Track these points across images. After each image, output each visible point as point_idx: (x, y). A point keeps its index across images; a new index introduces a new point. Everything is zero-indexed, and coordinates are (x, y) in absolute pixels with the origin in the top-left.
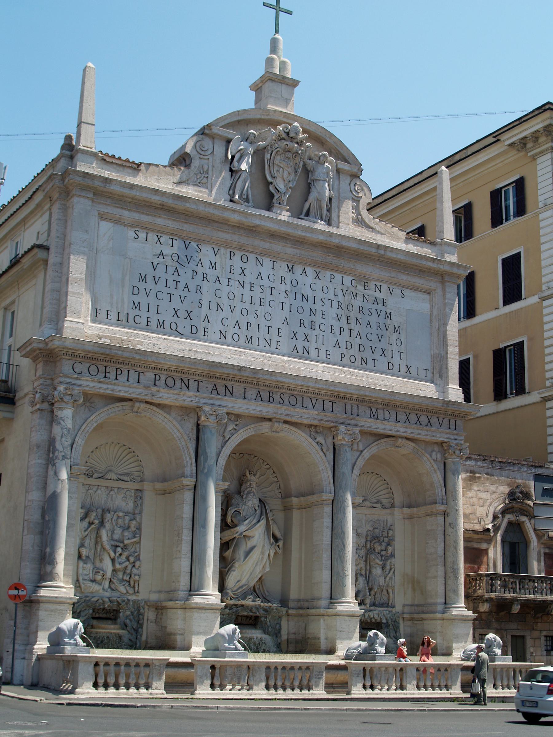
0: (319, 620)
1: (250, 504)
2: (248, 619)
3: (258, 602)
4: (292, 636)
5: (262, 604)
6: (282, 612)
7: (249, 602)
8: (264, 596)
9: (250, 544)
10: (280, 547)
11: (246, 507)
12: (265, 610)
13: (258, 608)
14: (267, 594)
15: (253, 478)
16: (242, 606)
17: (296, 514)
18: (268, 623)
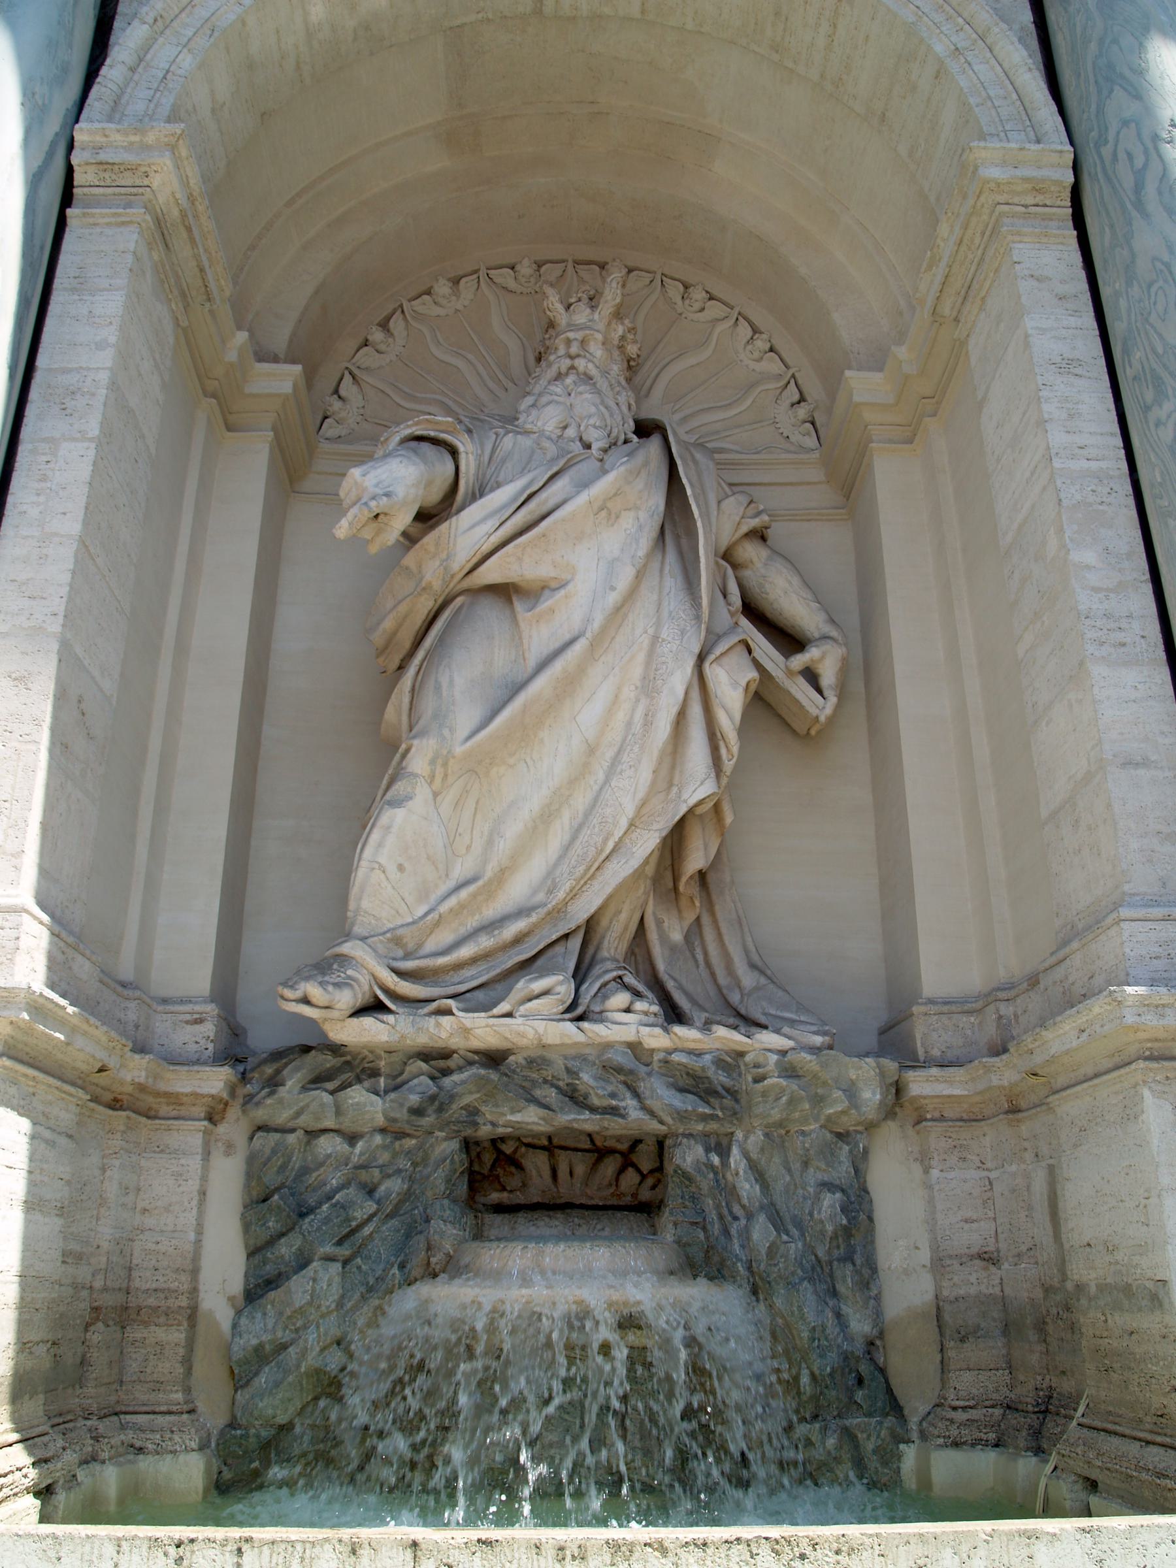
0: (1131, 1113)
1: (548, 419)
2: (609, 1167)
3: (628, 1023)
4: (973, 1282)
5: (656, 1039)
6: (851, 1092)
7: (532, 1021)
8: (735, 998)
9: (540, 631)
10: (828, 678)
11: (526, 442)
12: (694, 1084)
13: (628, 1069)
14: (748, 979)
15: (582, 315)
16: (494, 1059)
17: (890, 476)
18: (748, 1188)
